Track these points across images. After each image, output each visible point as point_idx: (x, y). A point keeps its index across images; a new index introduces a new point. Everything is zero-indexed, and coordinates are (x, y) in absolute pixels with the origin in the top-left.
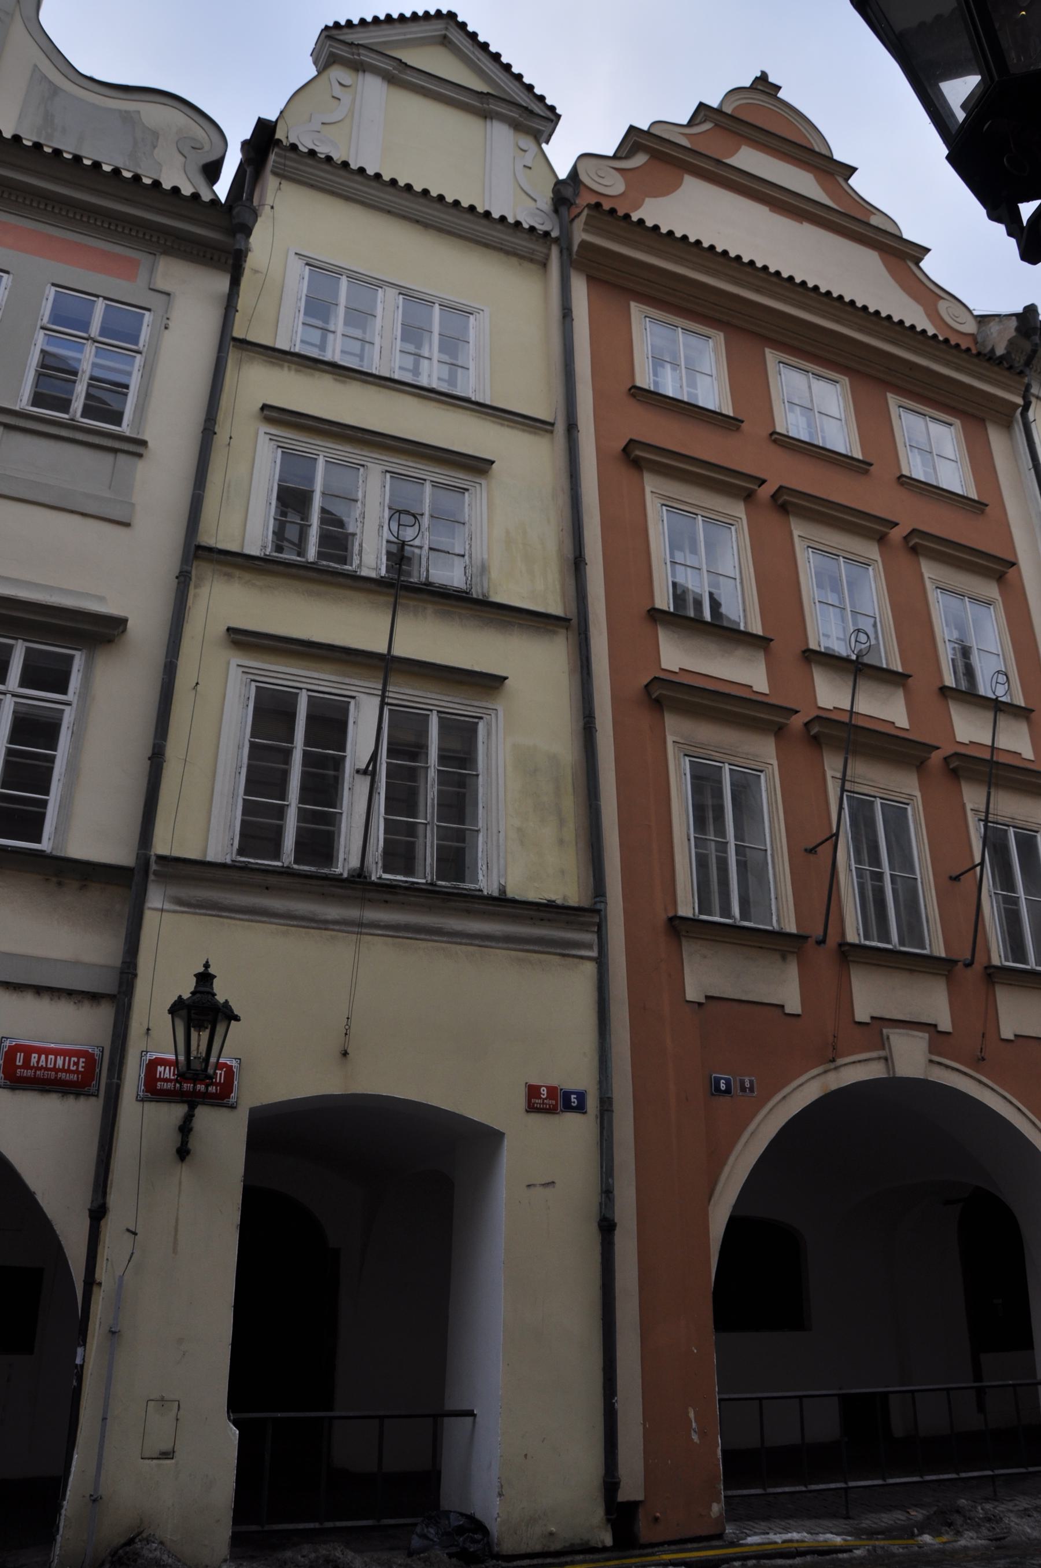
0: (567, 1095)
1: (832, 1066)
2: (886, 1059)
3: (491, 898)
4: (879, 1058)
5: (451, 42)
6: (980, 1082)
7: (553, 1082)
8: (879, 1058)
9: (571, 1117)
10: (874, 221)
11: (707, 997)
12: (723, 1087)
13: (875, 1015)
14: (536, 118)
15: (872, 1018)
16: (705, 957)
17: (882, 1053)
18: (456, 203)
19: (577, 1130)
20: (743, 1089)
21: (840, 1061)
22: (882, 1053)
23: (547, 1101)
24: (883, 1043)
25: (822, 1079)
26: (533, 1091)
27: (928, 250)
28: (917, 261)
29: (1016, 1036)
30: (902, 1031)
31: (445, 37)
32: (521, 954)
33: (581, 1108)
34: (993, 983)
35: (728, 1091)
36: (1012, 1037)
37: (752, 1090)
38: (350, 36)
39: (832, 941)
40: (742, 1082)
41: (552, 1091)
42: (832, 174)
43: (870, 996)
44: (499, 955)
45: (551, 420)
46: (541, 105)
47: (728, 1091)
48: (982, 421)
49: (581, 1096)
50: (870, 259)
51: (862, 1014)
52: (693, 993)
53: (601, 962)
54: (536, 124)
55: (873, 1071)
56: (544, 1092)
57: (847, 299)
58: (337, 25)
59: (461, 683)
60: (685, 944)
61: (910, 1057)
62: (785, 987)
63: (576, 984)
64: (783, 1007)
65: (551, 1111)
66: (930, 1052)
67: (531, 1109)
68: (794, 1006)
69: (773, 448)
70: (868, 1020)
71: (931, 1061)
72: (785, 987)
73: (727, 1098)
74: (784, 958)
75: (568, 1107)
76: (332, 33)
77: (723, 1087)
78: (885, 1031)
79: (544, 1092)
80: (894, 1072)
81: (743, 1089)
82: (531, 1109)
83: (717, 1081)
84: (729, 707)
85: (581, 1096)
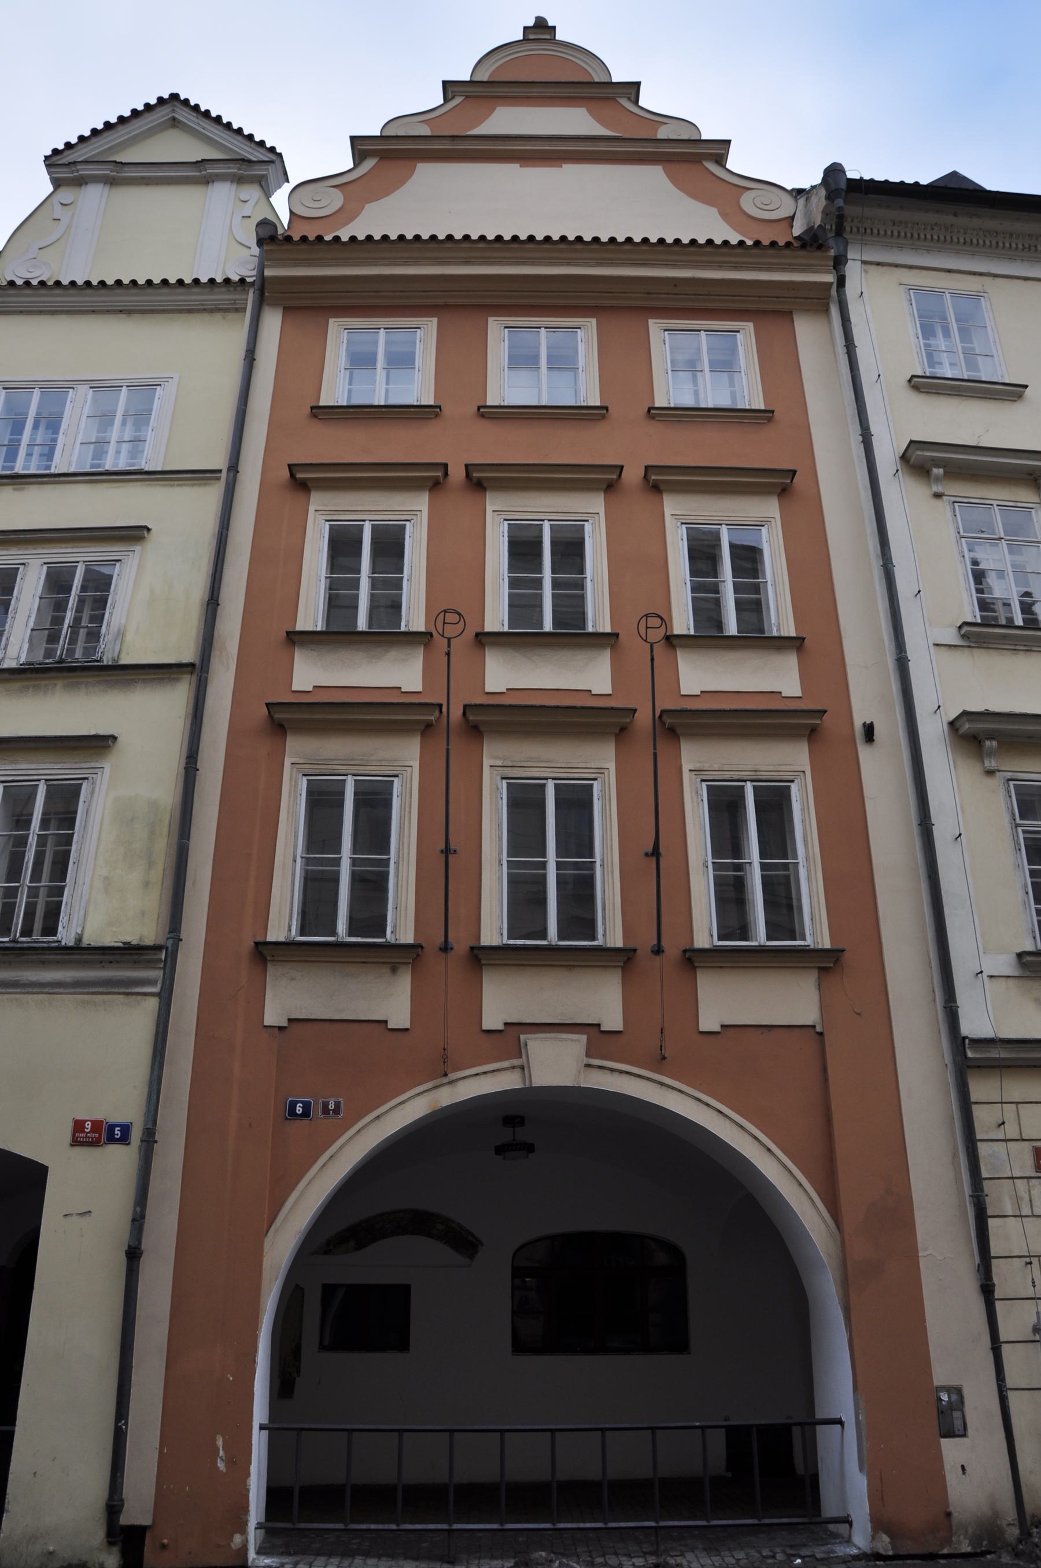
0: (111, 1127)
1: (445, 1080)
2: (522, 1068)
3: (66, 948)
5: (180, 122)
6: (662, 1084)
7: (98, 1117)
10: (662, 133)
11: (290, 1020)
12: (299, 1110)
13: (509, 1021)
14: (254, 163)
15: (506, 1024)
16: (293, 979)
17: (516, 1062)
18: (149, 282)
19: (120, 1159)
20: (326, 1110)
22: (516, 1062)
24: (518, 1050)
26: (78, 1126)
27: (729, 142)
28: (721, 160)
29: (722, 1026)
30: (552, 1035)
31: (174, 119)
32: (86, 997)
33: (125, 1139)
34: (694, 969)
35: (306, 1113)
37: (337, 1111)
40: (325, 1105)
41: (97, 1125)
42: (614, 99)
44: (67, 1000)
46: (262, 150)
47: (306, 1113)
48: (789, 315)
49: (126, 1129)
50: (652, 177)
51: (492, 1020)
52: (273, 1016)
53: (166, 998)
54: (258, 171)
55: (506, 1081)
56: (88, 1126)
57: (571, 238)
59: (75, 748)
60: (270, 967)
61: (556, 1065)
62: (393, 1002)
63: (136, 1019)
65: (94, 1143)
66: (588, 1055)
67: (75, 1142)
70: (501, 1027)
73: (305, 1122)
74: (394, 970)
75: (111, 1139)
77: (299, 1110)
78: (522, 1037)
79: (88, 1126)
80: (531, 1081)
81: (326, 1110)
82: (75, 1142)
83: (293, 1105)
84: (356, 717)
85: (126, 1129)
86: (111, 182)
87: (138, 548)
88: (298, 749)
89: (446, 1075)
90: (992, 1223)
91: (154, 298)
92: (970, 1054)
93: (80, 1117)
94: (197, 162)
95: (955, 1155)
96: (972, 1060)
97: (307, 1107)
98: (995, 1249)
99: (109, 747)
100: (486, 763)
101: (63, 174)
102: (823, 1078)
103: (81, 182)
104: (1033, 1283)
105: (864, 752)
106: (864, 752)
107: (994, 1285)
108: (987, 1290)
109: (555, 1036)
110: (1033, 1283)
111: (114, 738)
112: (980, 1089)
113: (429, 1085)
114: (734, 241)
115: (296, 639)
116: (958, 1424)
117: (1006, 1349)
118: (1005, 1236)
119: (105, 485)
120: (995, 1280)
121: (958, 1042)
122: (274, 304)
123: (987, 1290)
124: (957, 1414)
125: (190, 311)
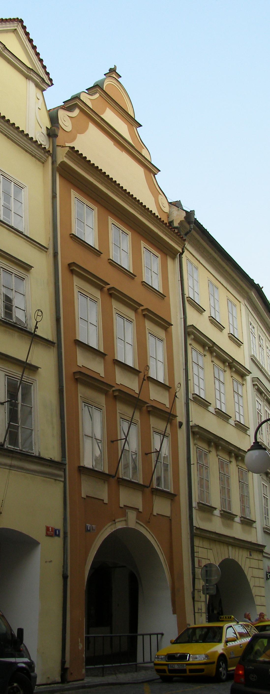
0: (56, 530)
2: (126, 520)
3: (35, 457)
5: (18, 33)
6: (147, 530)
7: (52, 526)
9: (56, 538)
10: (144, 152)
14: (43, 82)
15: (124, 506)
20: (93, 529)
23: (52, 533)
24: (125, 515)
26: (48, 529)
28: (155, 174)
33: (59, 536)
35: (89, 531)
39: (151, 487)
42: (133, 126)
43: (127, 497)
45: (47, 247)
46: (47, 76)
50: (140, 171)
53: (65, 482)
54: (44, 86)
60: (82, 476)
61: (132, 521)
64: (103, 500)
65: (51, 536)
67: (47, 535)
68: (106, 501)
69: (109, 265)
71: (136, 522)
74: (104, 482)
78: (127, 510)
79: (50, 529)
82: (47, 535)
91: (21, 139)
92: (195, 531)
93: (49, 526)
94: (6, 48)
114: (165, 222)
119: (12, 234)
125: (8, 138)
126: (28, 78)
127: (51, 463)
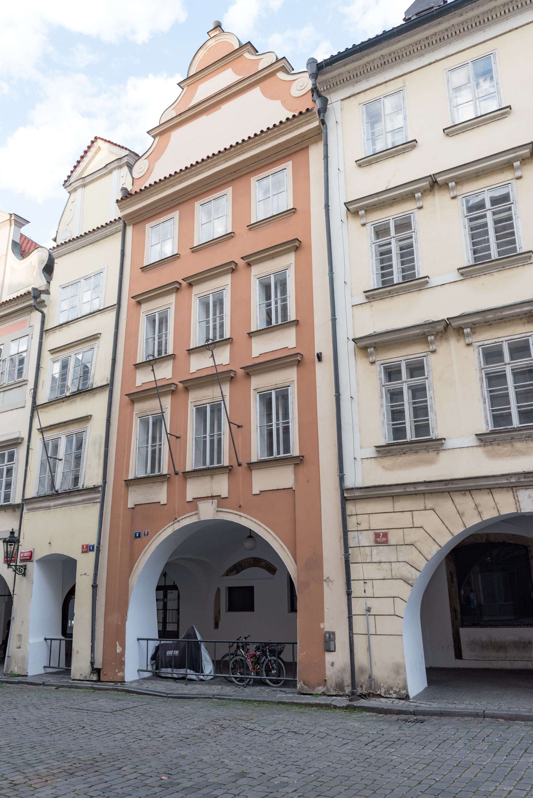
4: (195, 514)
7: (87, 544)
8: (195, 514)
12: (137, 535)
16: (135, 491)
21: (178, 519)
24: (197, 509)
25: (172, 526)
33: (93, 550)
35: (139, 536)
36: (258, 493)
37: (147, 535)
38: (72, 180)
41: (87, 546)
49: (93, 546)
51: (189, 498)
52: (130, 505)
56: (85, 546)
58: (66, 181)
60: (130, 488)
61: (207, 512)
65: (86, 552)
66: (218, 507)
70: (192, 500)
71: (217, 511)
72: (160, 494)
73: (139, 539)
75: (90, 550)
76: (66, 183)
81: (145, 535)
82: (83, 552)
83: (136, 535)
85: (93, 546)
86: (84, 186)
87: (97, 342)
88: (139, 407)
89: (176, 519)
90: (352, 566)
95: (341, 538)
96: (347, 496)
97: (139, 534)
98: (353, 577)
99: (90, 419)
100: (190, 401)
101: (70, 189)
102: (296, 509)
103: (75, 190)
104: (365, 591)
105: (318, 365)
106: (318, 365)
107: (352, 592)
108: (349, 594)
109: (207, 502)
110: (365, 591)
111: (91, 416)
112: (351, 508)
113: (172, 523)
115: (138, 366)
116: (332, 648)
117: (354, 618)
118: (356, 571)
120: (353, 589)
121: (343, 490)
122: (129, 225)
123: (349, 594)
124: (332, 643)
126: (110, 172)
127: (94, 489)
